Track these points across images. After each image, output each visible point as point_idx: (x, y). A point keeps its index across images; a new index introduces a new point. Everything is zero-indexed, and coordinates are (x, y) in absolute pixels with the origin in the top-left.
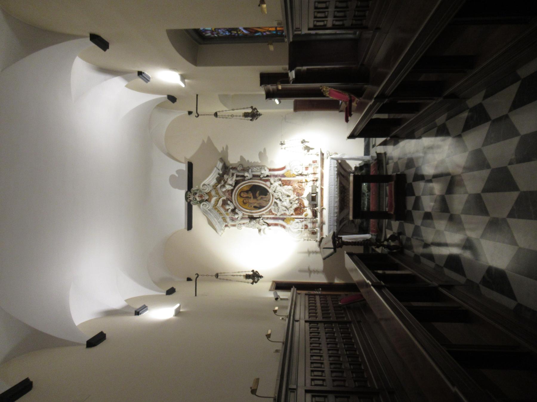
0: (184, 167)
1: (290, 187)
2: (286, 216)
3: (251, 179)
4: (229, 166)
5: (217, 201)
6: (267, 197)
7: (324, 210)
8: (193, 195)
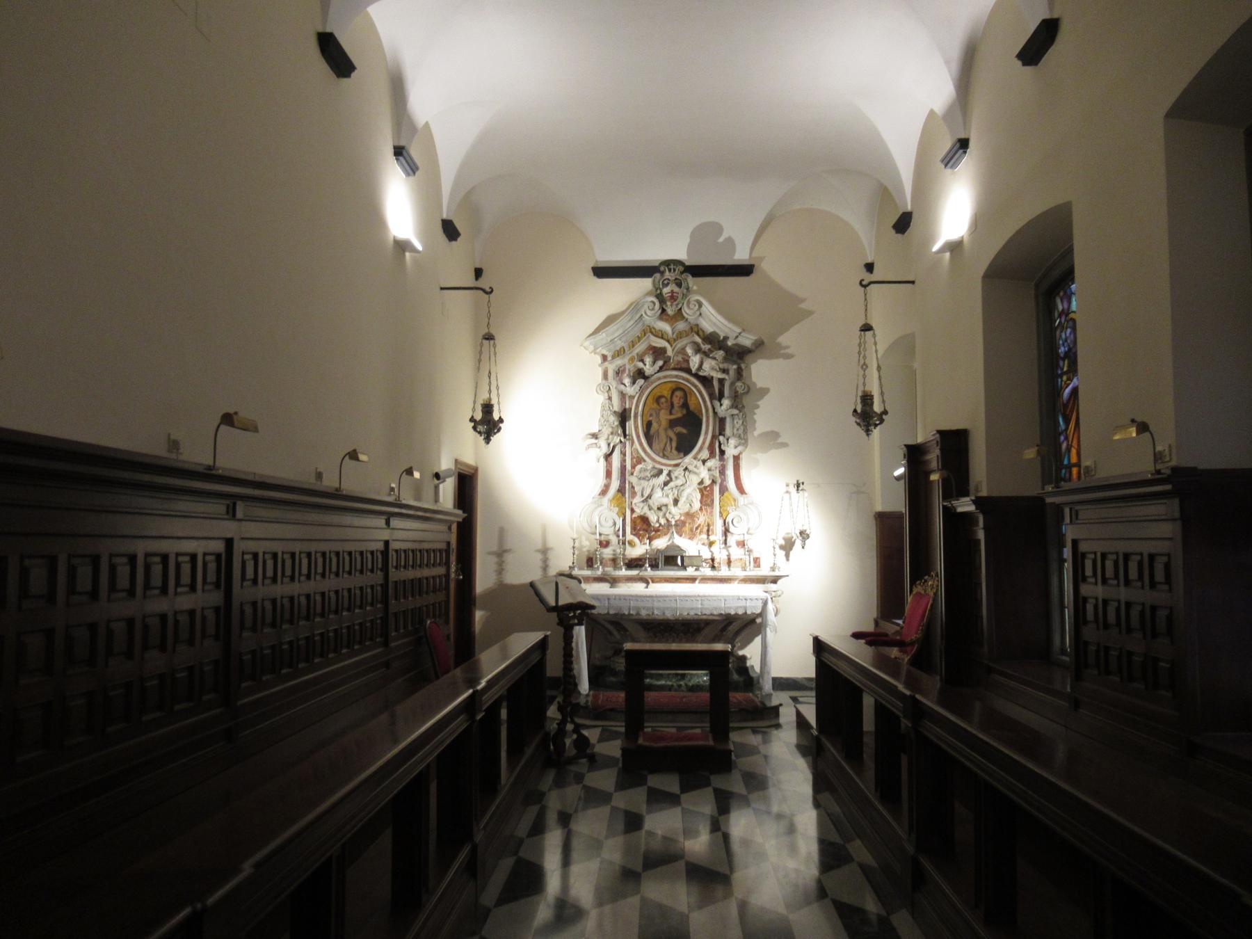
0: (741, 256)
1: (697, 505)
3: (715, 413)
5: (662, 335)
6: (675, 452)
7: (645, 585)
8: (676, 279)
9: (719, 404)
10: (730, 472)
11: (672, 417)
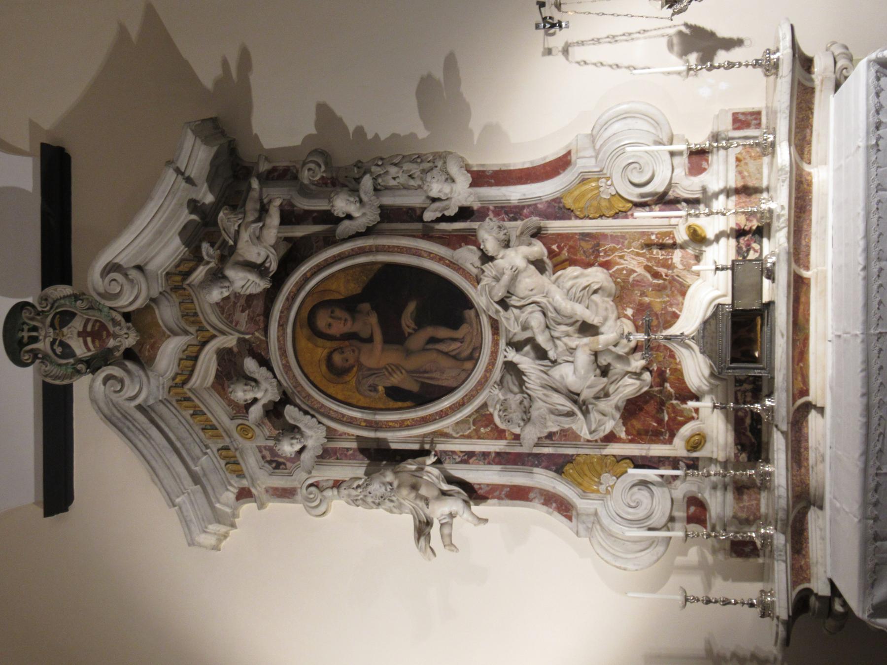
1: (596, 276)
2: (576, 447)
3: (369, 232)
4: (257, 163)
5: (188, 358)
6: (459, 334)
7: (813, 415)
8: (52, 325)
9: (346, 223)
10: (515, 194)
11: (378, 337)
